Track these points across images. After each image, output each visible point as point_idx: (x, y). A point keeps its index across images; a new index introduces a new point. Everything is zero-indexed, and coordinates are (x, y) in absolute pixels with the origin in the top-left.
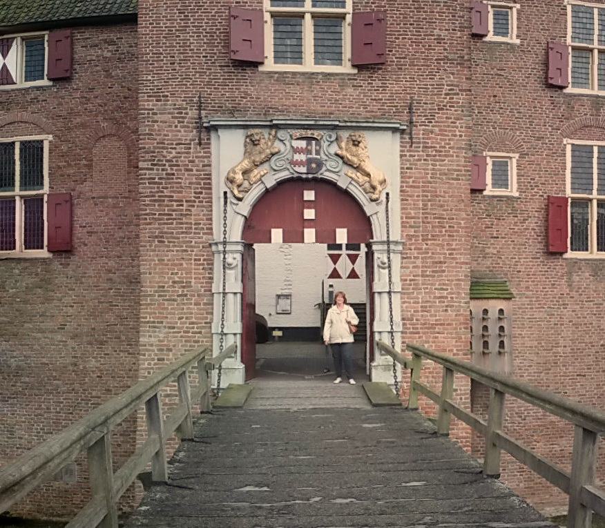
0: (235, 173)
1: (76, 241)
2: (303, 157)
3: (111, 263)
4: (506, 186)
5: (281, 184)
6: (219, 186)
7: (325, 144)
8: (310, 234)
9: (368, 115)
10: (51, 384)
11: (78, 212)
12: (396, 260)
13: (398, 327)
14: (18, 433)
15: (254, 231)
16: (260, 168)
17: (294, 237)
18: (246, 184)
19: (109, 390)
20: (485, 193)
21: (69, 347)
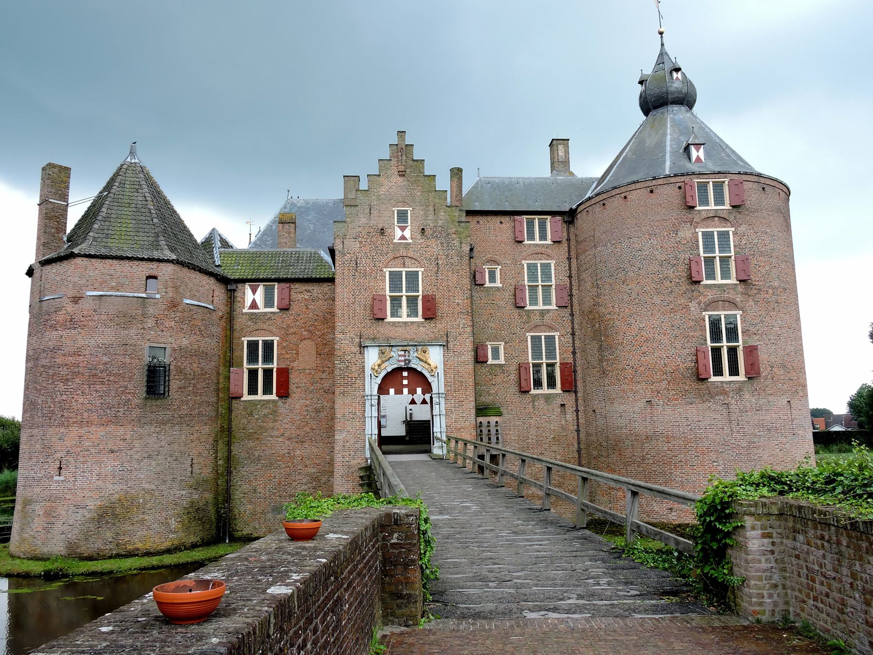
0: (375, 366)
1: (290, 391)
2: (403, 358)
3: (308, 402)
4: (499, 359)
5: (394, 370)
6: (368, 371)
7: (411, 353)
8: (405, 391)
9: (429, 339)
10: (277, 464)
11: (291, 376)
12: (442, 401)
13: (444, 429)
14: (259, 490)
15: (383, 389)
16: (385, 364)
17: (399, 392)
18: (379, 370)
19: (306, 466)
20: (488, 363)
21: (286, 445)
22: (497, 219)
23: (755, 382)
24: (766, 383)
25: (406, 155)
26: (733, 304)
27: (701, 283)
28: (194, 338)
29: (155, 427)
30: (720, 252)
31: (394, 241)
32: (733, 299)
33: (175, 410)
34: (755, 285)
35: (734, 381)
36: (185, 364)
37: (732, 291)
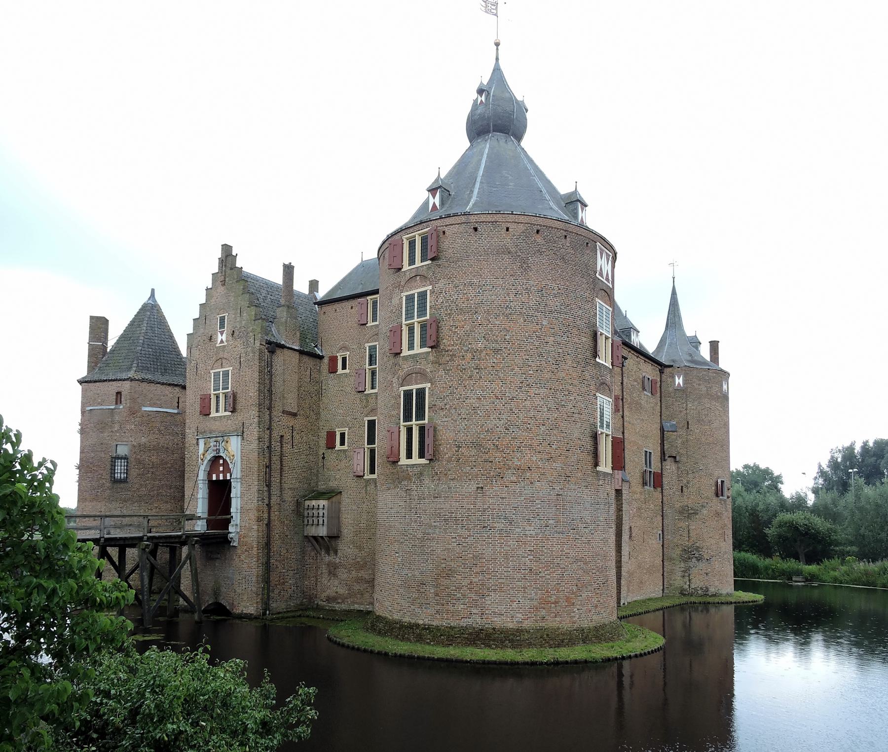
22: (347, 304)
23: (437, 464)
24: (450, 466)
25: (225, 266)
26: (422, 375)
27: (401, 355)
28: (151, 437)
29: (120, 504)
30: (419, 317)
31: (217, 345)
32: (424, 370)
33: (134, 491)
34: (448, 351)
35: (417, 464)
36: (144, 457)
37: (424, 362)
